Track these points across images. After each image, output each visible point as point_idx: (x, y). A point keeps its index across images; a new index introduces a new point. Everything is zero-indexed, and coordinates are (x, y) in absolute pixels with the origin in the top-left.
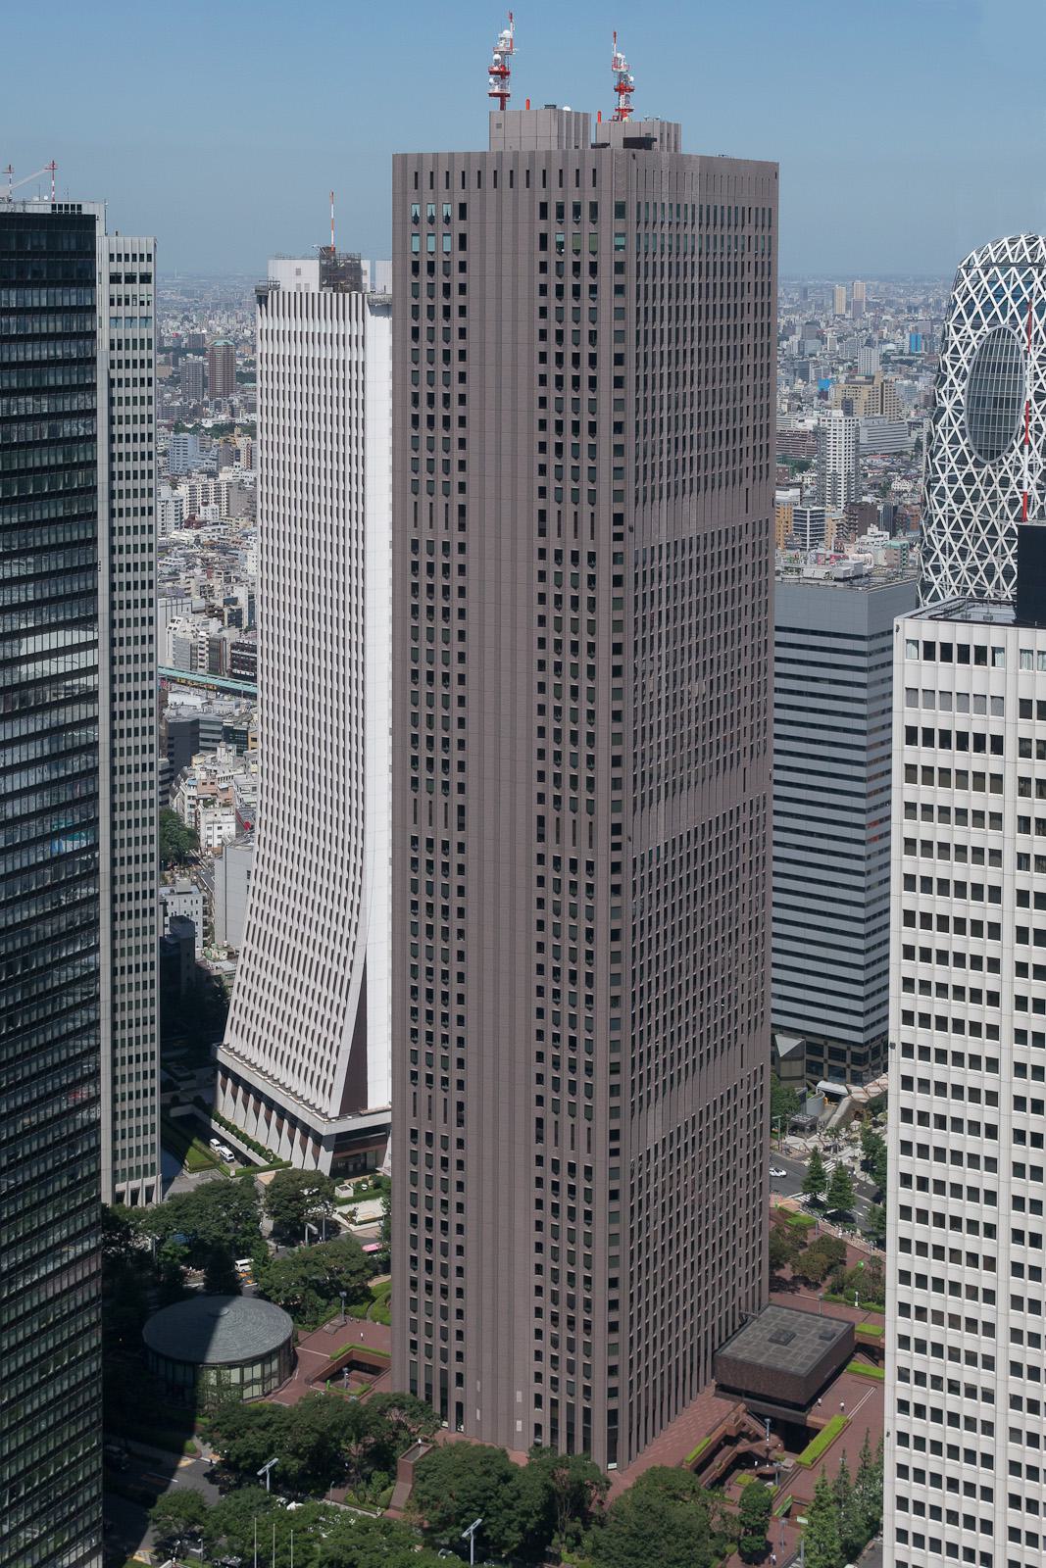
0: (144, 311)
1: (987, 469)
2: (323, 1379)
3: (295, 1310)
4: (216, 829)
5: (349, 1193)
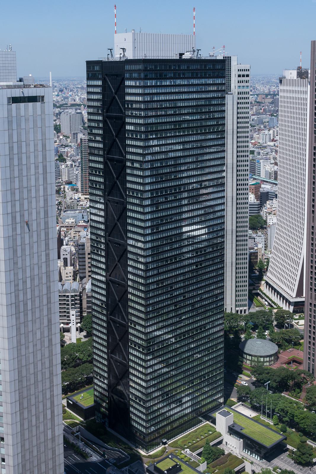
0: (247, 84)
2: (285, 363)
3: (280, 346)
4: (272, 220)
5: (297, 317)
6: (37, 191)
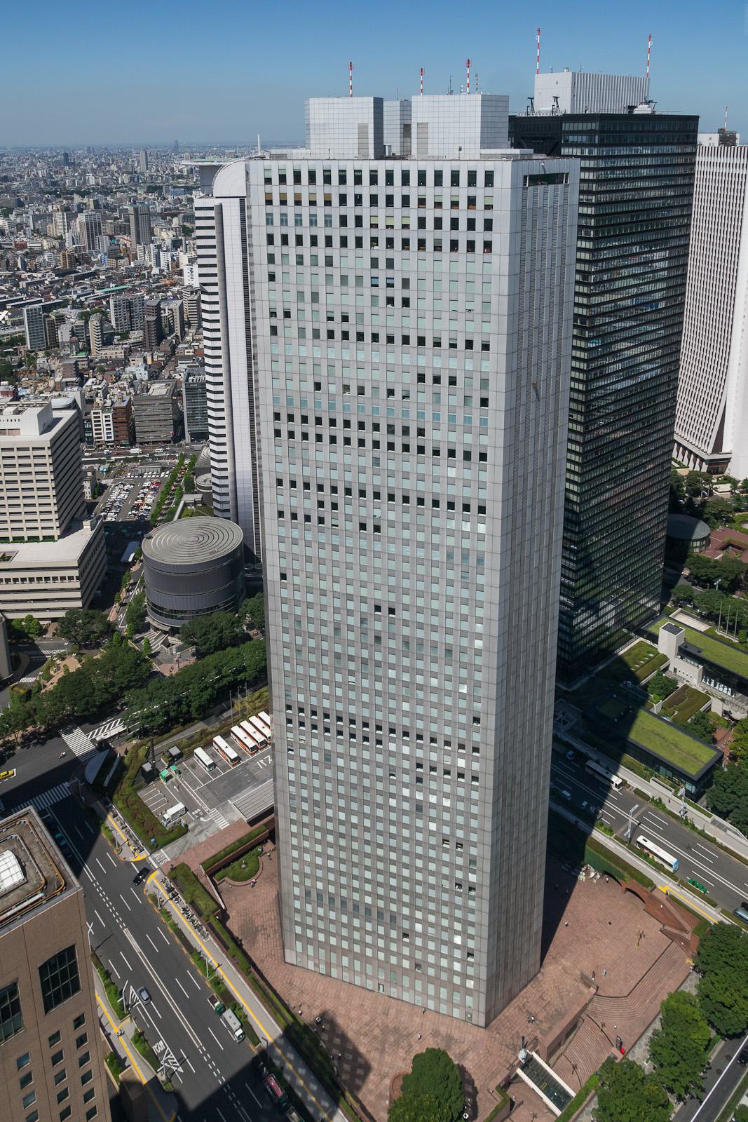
6: (550, 332)
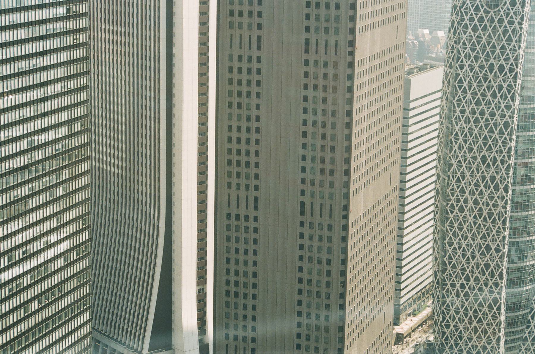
1: (492, 14)
